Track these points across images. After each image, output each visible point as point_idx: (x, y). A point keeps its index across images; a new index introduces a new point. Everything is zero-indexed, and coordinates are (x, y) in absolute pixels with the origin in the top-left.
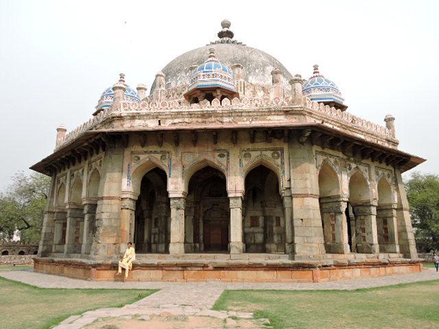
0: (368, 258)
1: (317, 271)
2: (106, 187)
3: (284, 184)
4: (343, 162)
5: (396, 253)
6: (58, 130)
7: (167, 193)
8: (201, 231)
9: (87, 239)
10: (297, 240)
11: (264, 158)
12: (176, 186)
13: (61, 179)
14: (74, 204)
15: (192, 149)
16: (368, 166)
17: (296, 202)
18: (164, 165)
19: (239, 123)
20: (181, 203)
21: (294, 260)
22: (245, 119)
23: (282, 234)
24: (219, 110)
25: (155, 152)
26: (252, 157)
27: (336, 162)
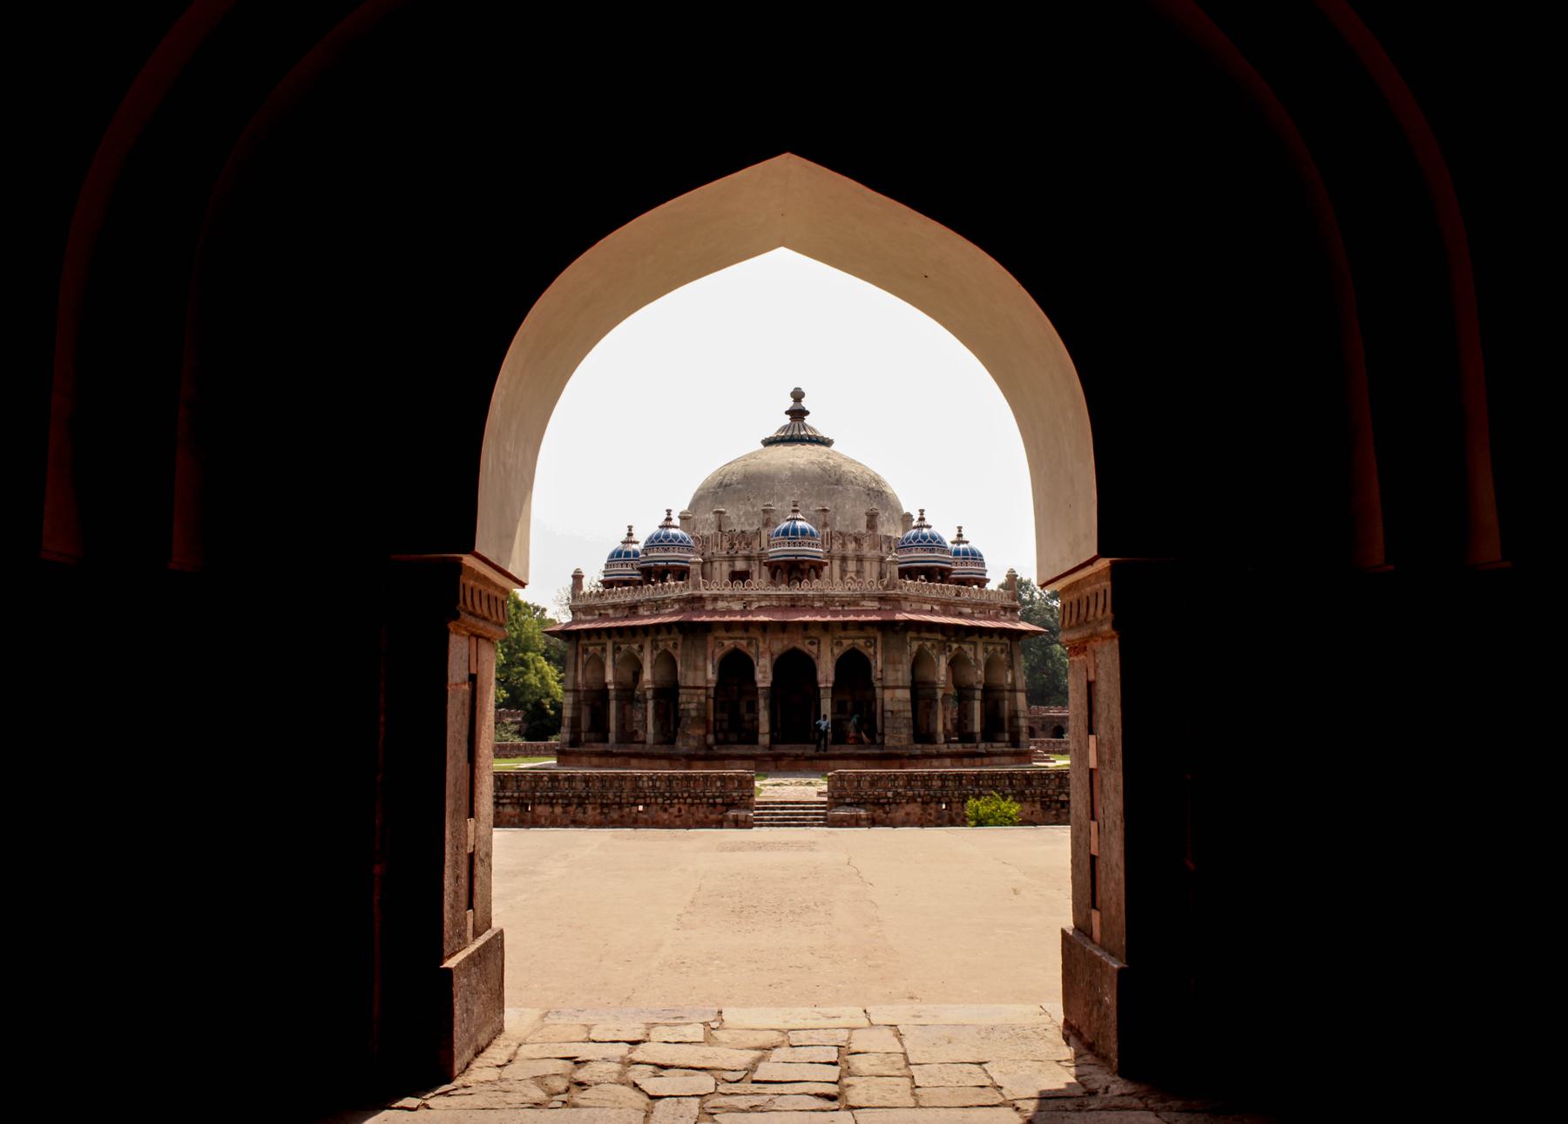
0: (964, 747)
1: (906, 761)
2: (690, 675)
3: (876, 674)
4: (942, 644)
5: (1004, 741)
7: (755, 683)
8: (779, 718)
11: (856, 646)
12: (763, 676)
13: (591, 648)
14: (620, 683)
15: (781, 636)
16: (975, 644)
18: (752, 651)
19: (831, 608)
21: (882, 749)
22: (837, 604)
25: (742, 638)
26: (845, 645)
27: (933, 646)
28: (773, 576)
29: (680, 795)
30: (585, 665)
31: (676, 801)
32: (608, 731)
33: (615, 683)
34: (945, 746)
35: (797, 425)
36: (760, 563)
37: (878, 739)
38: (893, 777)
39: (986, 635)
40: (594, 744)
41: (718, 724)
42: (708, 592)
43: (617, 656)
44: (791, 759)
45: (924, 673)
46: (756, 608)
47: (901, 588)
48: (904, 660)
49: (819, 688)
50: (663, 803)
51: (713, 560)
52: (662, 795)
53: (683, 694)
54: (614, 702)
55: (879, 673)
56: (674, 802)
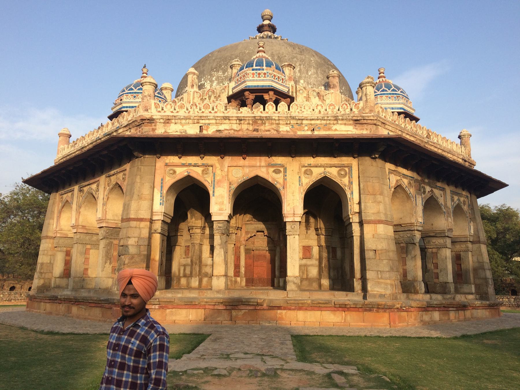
0: (444, 299)
2: (134, 205)
4: (418, 184)
5: (472, 294)
6: (60, 135)
10: (369, 275)
11: (328, 175)
13: (65, 196)
14: (84, 227)
18: (207, 181)
22: (306, 128)
24: (275, 116)
25: (195, 165)
26: (315, 174)
27: (410, 183)
34: (428, 296)
37: (357, 285)
41: (182, 269)
42: (160, 114)
46: (213, 132)
48: (386, 192)
49: (286, 222)
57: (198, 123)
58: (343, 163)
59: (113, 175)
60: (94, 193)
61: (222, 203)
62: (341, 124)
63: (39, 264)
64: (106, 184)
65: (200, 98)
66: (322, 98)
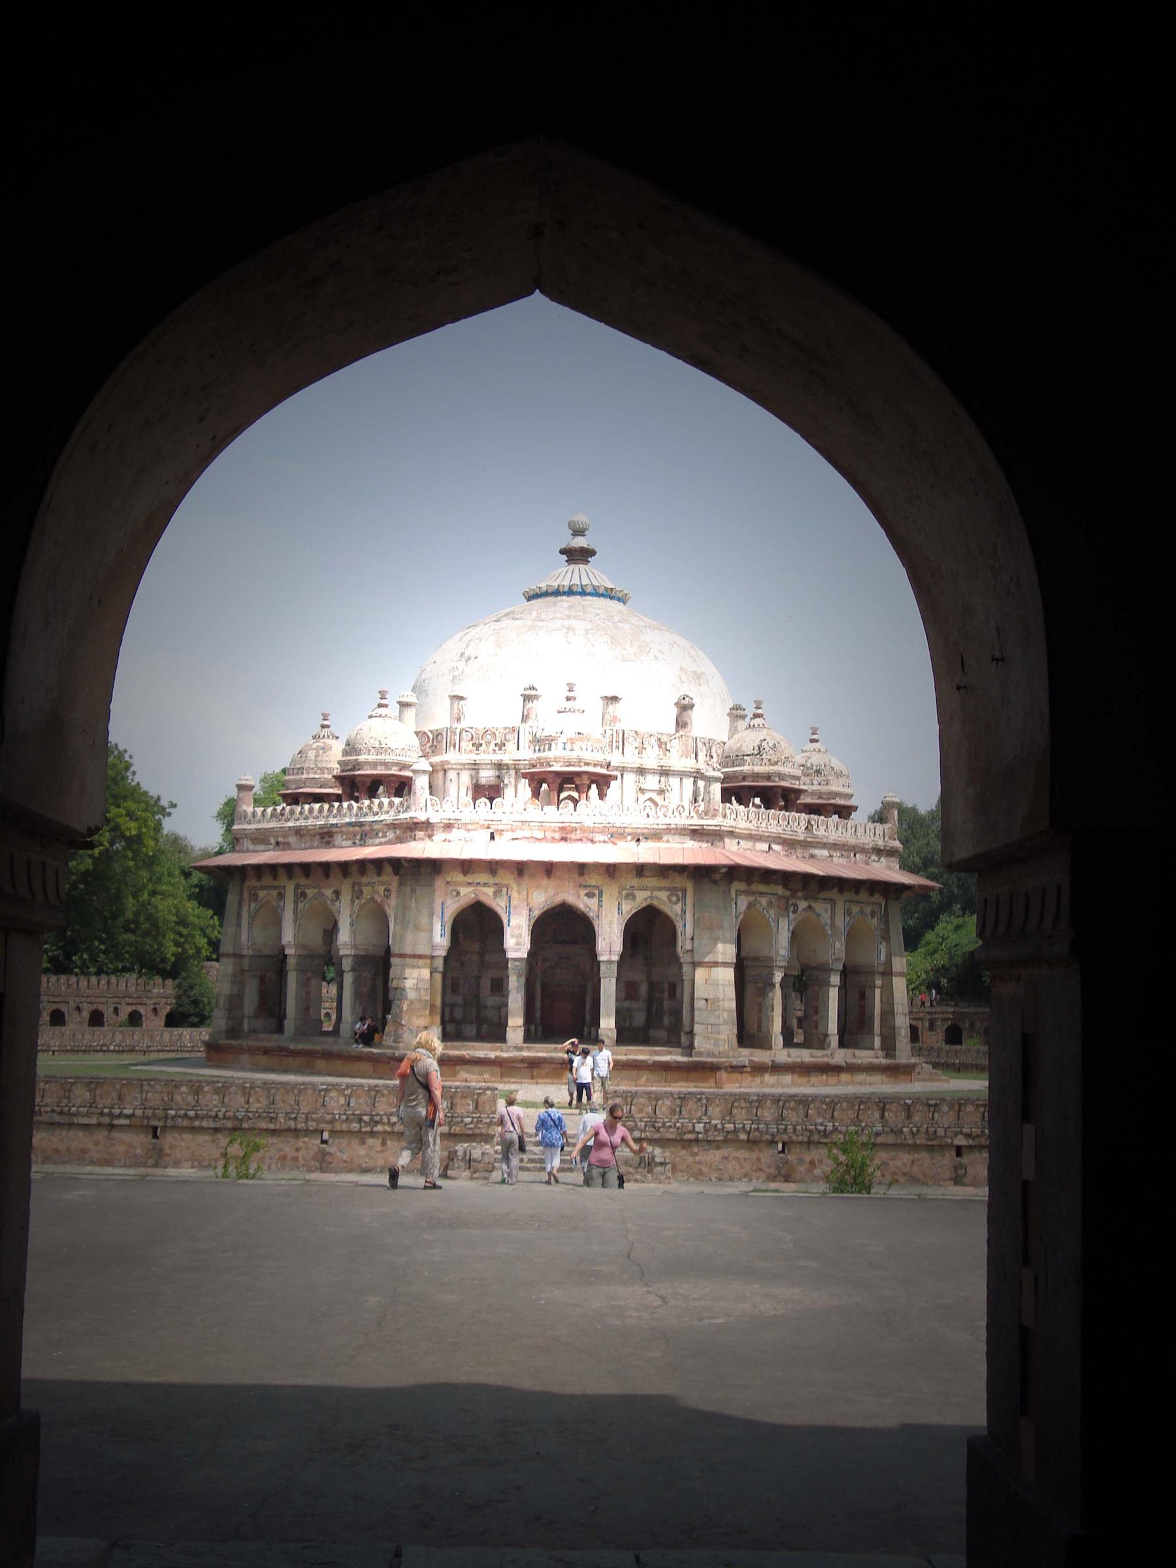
0: (811, 1056)
1: (723, 1075)
2: (409, 938)
5: (873, 1049)
7: (504, 952)
8: (538, 1004)
9: (352, 1014)
11: (655, 903)
13: (262, 894)
14: (304, 946)
15: (545, 882)
16: (833, 902)
17: (700, 974)
18: (499, 906)
20: (523, 966)
21: (691, 1056)
22: (629, 838)
23: (677, 1014)
24: (588, 822)
25: (485, 885)
27: (770, 904)
28: (536, 794)
29: (385, 1120)
30: (252, 918)
31: (379, 1128)
32: (281, 1018)
33: (296, 946)
34: (785, 1052)
35: (576, 571)
36: (516, 773)
37: (684, 1039)
38: (704, 1101)
39: (850, 890)
40: (261, 1036)
43: (300, 905)
44: (553, 1066)
45: (754, 945)
47: (725, 816)
48: (726, 924)
49: (599, 962)
50: (360, 1131)
51: (446, 767)
52: (360, 1121)
53: (397, 966)
54: (295, 973)
55: (688, 942)
56: (375, 1129)
57: (488, 828)
58: (676, 885)
59: (367, 886)
60: (329, 902)
61: (520, 936)
62: (675, 834)
63: (222, 998)
64: (354, 897)
65: (471, 743)
66: (663, 746)
